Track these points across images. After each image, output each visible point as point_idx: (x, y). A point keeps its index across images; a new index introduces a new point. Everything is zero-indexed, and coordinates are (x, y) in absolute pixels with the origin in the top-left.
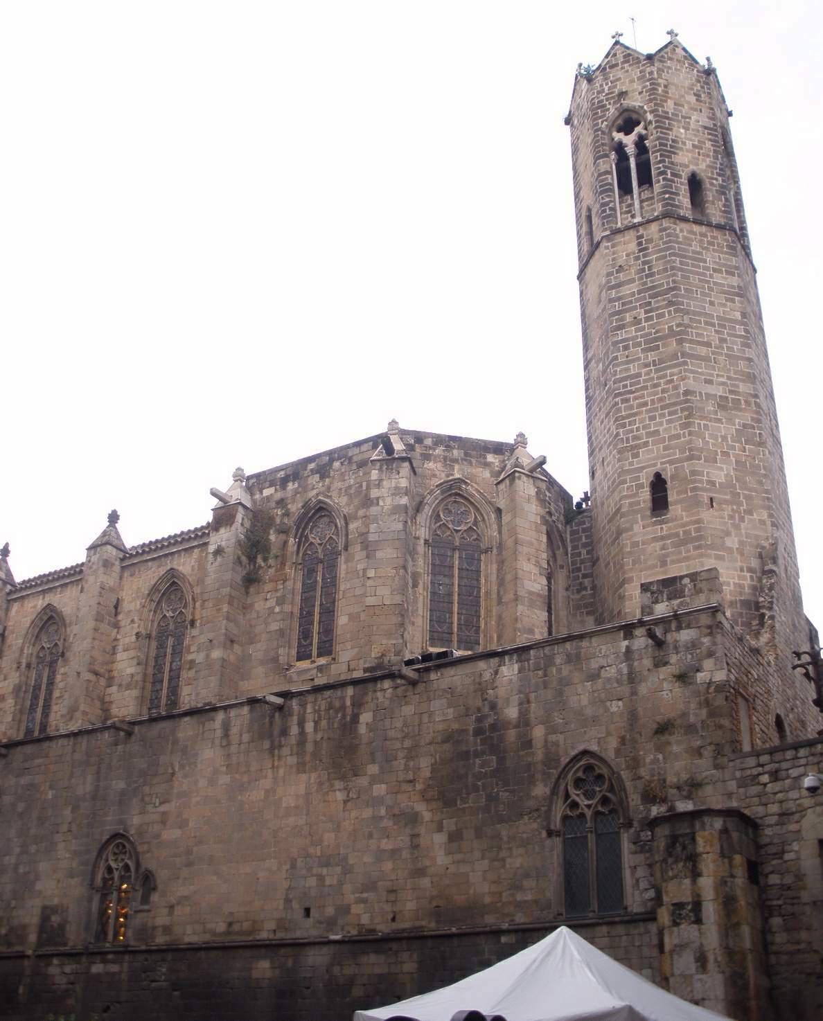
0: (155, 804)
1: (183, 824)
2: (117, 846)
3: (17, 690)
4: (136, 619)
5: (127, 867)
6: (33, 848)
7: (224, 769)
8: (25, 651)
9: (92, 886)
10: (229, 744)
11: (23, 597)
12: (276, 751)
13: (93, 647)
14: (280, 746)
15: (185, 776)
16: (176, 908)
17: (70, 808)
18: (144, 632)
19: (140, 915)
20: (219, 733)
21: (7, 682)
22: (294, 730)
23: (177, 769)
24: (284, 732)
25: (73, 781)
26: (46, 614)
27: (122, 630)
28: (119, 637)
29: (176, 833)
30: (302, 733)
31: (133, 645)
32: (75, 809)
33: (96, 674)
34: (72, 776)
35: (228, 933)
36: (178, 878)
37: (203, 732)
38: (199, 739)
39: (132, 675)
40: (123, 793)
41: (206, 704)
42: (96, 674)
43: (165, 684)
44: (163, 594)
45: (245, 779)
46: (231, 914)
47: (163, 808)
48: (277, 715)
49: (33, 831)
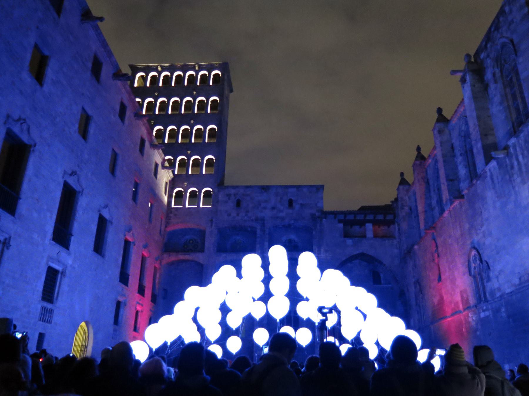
7: (497, 199)
14: (513, 175)
20: (490, 182)
22: (516, 164)
24: (512, 167)
30: (519, 163)
32: (458, 243)
33: (452, 180)
35: (520, 284)
39: (465, 174)
42: (452, 180)
46: (519, 273)
47: (483, 229)
48: (507, 160)
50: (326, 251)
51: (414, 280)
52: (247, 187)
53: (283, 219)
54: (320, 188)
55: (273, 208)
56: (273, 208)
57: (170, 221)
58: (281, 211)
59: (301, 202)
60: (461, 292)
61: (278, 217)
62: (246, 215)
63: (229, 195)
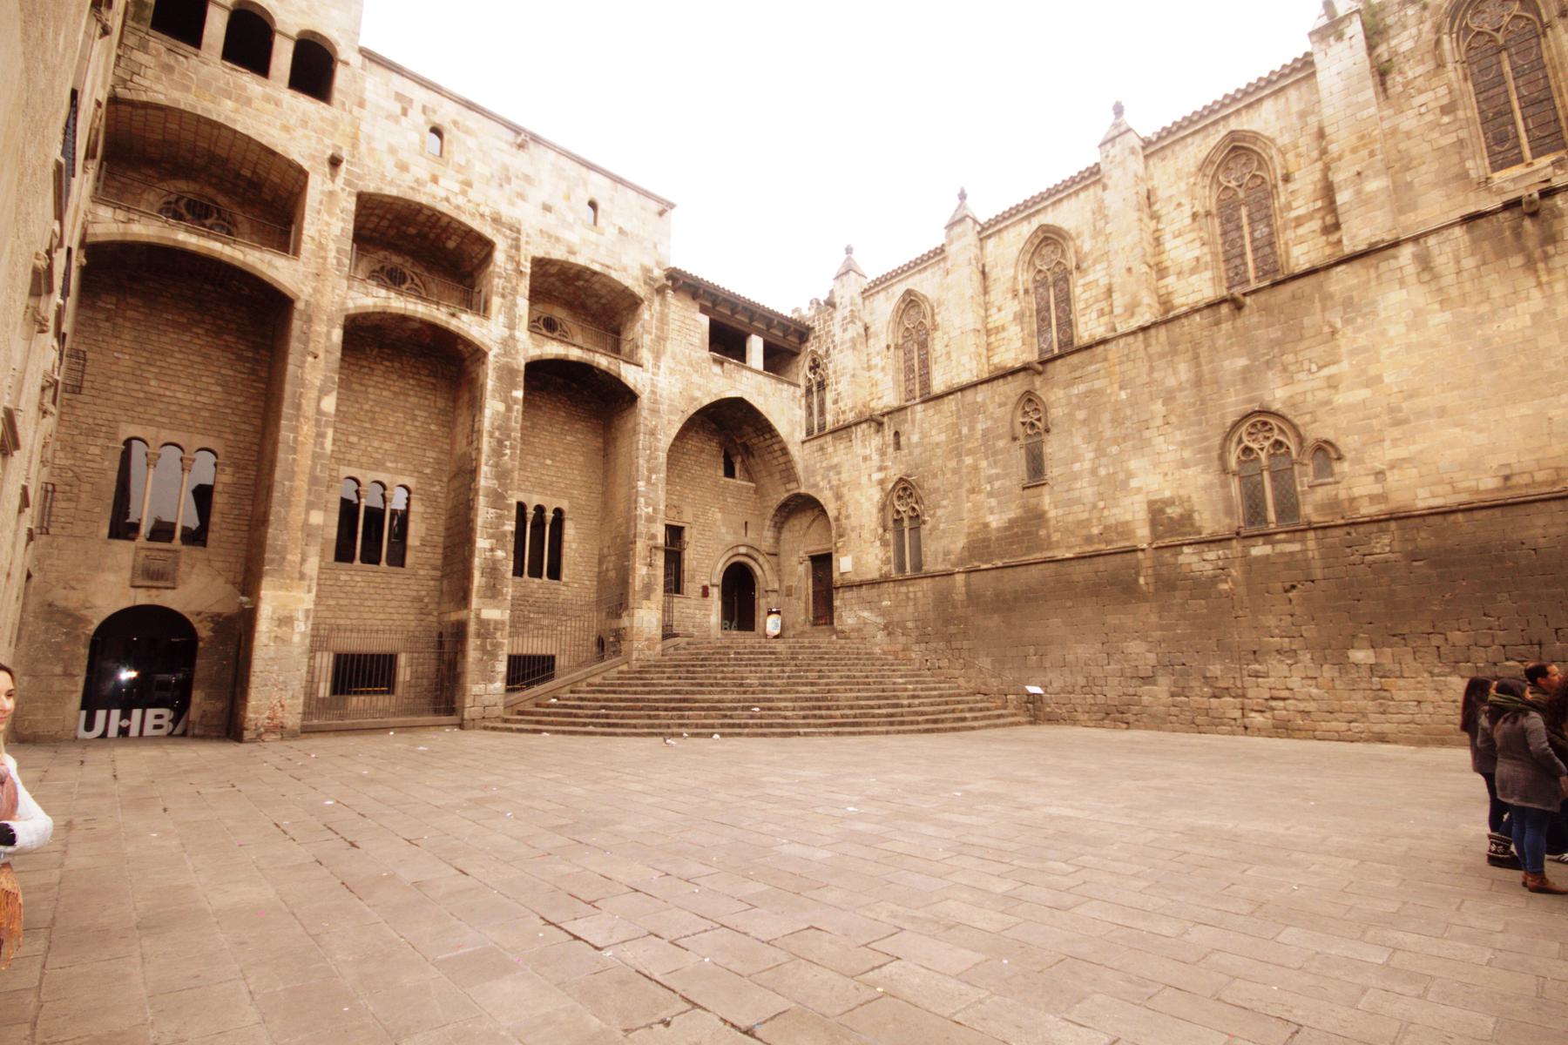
0: (1309, 370)
1: (1374, 381)
2: (1254, 425)
3: (1019, 317)
4: (1183, 201)
5: (1278, 444)
6: (1114, 449)
7: (1437, 306)
8: (1020, 278)
9: (1225, 470)
10: (1436, 277)
11: (1000, 231)
12: (1541, 266)
13: (1142, 239)
15: (1359, 330)
16: (1388, 474)
17: (1160, 401)
18: (1202, 211)
19: (1319, 489)
20: (1411, 270)
21: (1003, 313)
23: (1339, 324)
25: (1156, 375)
26: (1037, 236)
27: (1164, 219)
28: (1160, 226)
29: (1365, 393)
31: (1188, 229)
32: (1169, 399)
34: (1152, 369)
36: (1383, 441)
37: (1378, 277)
38: (1373, 283)
39: (1198, 259)
40: (1246, 370)
41: (1371, 245)
43: (1249, 257)
44: (1219, 166)
45: (1484, 308)
47: (1326, 372)
49: (1108, 433)
50: (672, 372)
51: (877, 476)
52: (470, 106)
53: (572, 252)
54: (665, 208)
55: (547, 208)
56: (547, 208)
57: (136, 78)
58: (570, 227)
59: (620, 222)
60: (1151, 504)
61: (558, 239)
62: (464, 193)
63: (406, 105)
